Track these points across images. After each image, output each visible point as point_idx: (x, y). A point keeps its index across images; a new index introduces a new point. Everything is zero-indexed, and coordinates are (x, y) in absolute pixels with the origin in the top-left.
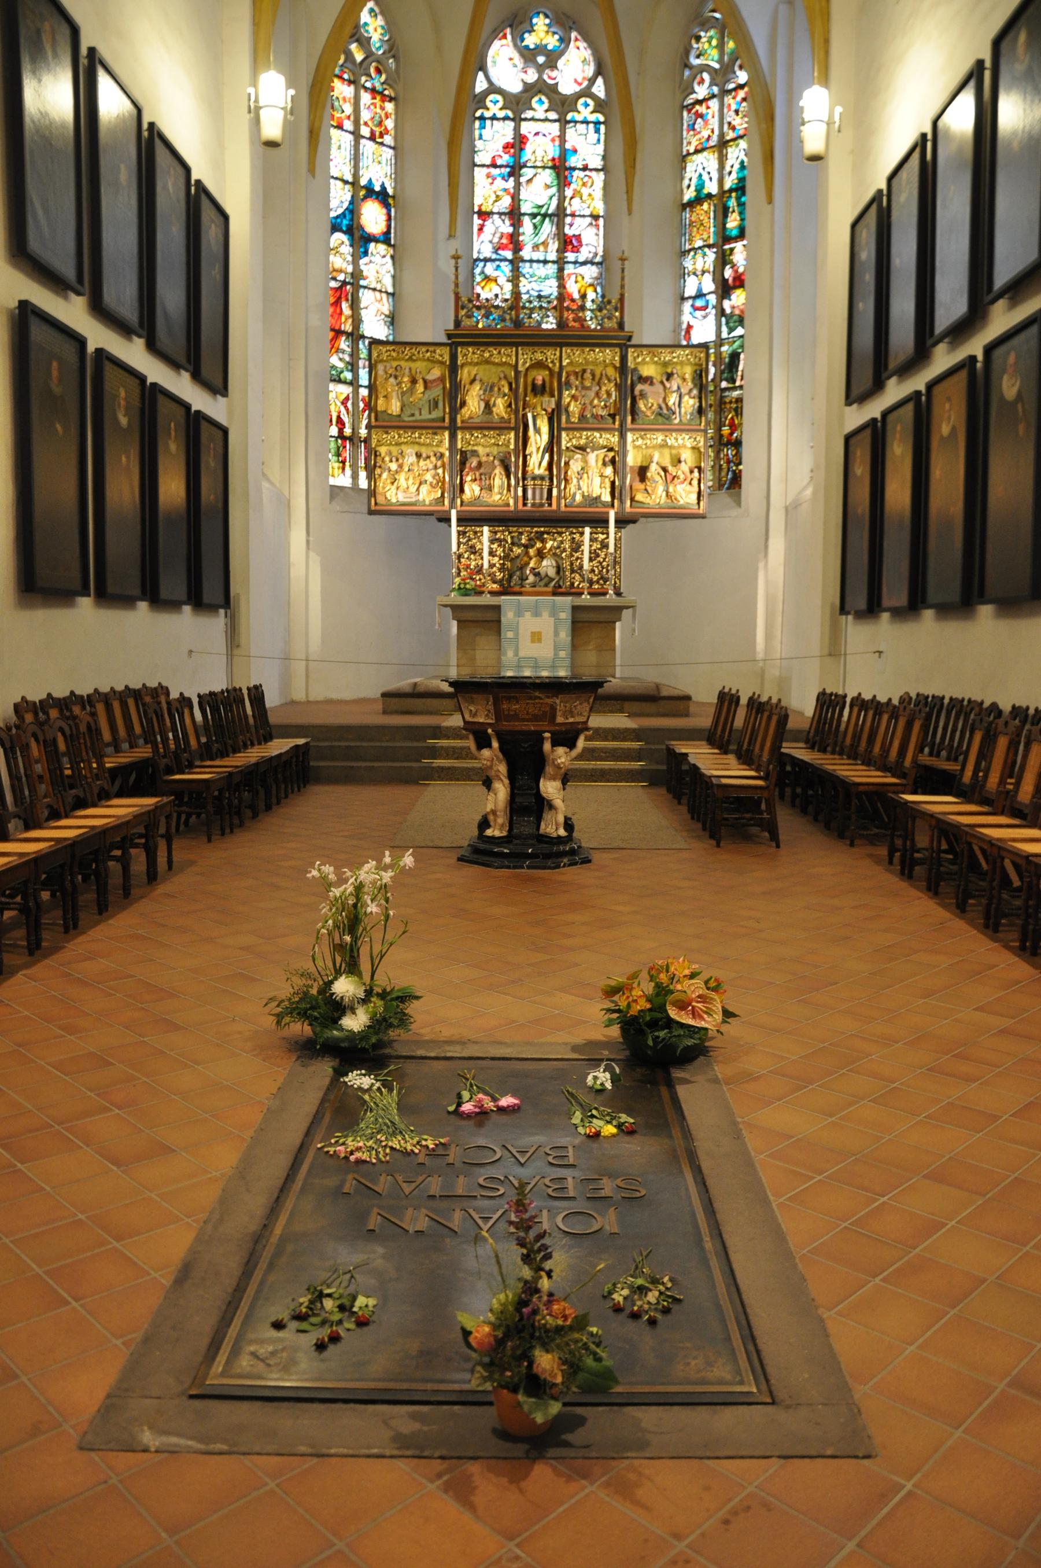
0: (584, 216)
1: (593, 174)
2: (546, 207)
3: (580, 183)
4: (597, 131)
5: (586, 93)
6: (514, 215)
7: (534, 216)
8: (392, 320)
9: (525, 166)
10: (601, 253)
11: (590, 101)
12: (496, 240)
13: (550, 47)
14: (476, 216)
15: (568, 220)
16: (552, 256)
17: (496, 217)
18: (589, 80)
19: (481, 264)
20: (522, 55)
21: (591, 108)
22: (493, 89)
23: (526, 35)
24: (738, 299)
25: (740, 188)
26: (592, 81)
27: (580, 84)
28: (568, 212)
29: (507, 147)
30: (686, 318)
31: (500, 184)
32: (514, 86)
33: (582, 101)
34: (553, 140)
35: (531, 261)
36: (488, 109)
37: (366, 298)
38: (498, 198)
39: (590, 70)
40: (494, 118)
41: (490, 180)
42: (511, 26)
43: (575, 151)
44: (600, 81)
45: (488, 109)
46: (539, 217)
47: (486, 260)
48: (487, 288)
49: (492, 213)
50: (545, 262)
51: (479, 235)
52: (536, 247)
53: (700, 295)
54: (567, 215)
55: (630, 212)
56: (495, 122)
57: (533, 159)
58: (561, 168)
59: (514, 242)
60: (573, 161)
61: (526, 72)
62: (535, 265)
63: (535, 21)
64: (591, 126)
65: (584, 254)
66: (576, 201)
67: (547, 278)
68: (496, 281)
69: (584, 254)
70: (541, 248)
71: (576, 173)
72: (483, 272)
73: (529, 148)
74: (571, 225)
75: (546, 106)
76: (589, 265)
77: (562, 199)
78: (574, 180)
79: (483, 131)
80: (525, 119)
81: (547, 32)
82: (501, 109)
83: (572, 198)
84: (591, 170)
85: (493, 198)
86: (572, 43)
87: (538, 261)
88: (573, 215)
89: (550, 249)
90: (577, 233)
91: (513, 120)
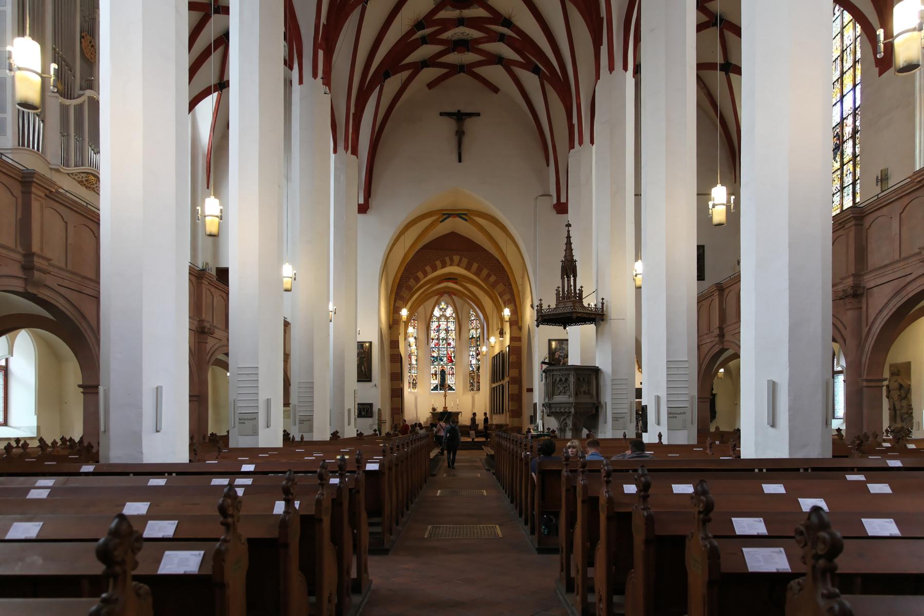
5: (452, 316)
6: (438, 339)
8: (416, 360)
16: (445, 347)
22: (434, 316)
24: (479, 357)
25: (479, 337)
26: (452, 314)
29: (437, 327)
30: (470, 359)
31: (436, 333)
32: (438, 316)
37: (413, 357)
39: (452, 312)
40: (434, 321)
52: (442, 345)
53: (473, 355)
55: (460, 339)
58: (447, 331)
59: (438, 344)
60: (449, 329)
65: (451, 346)
69: (451, 346)
77: (447, 335)
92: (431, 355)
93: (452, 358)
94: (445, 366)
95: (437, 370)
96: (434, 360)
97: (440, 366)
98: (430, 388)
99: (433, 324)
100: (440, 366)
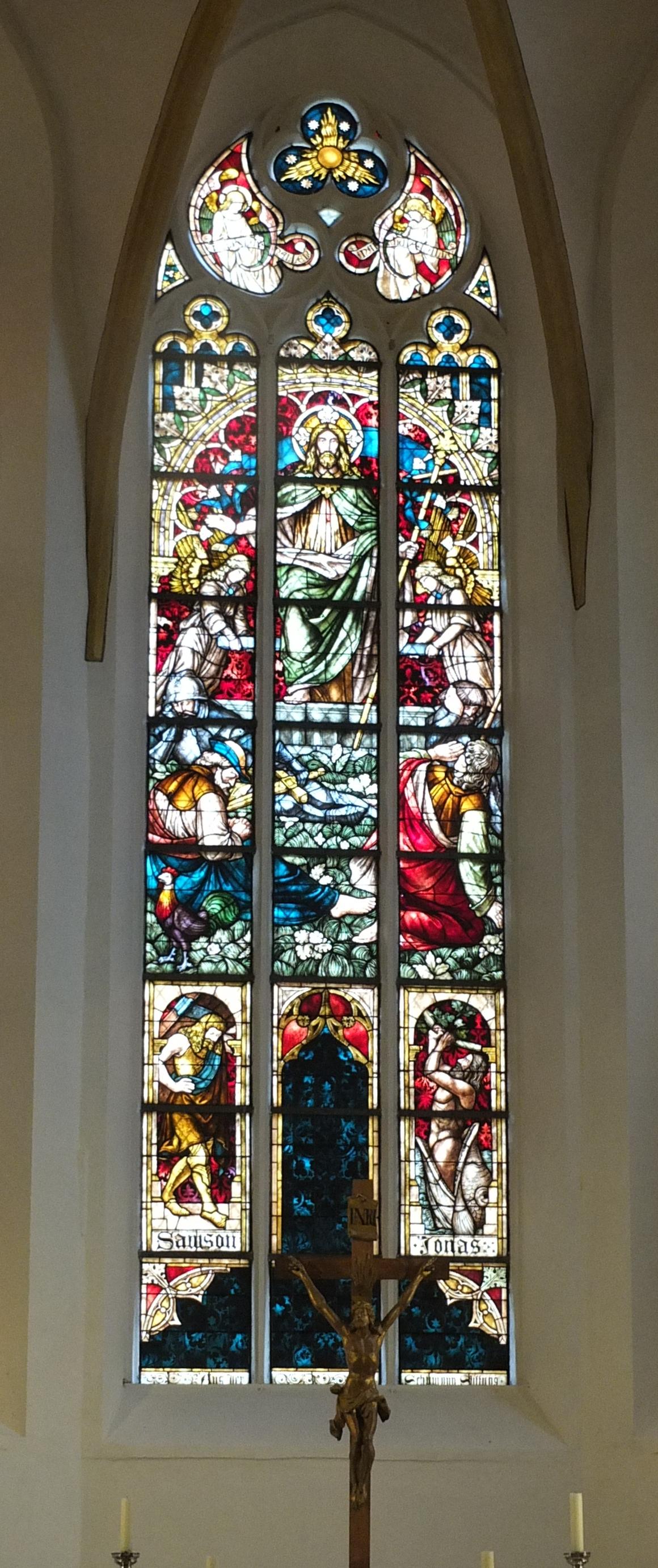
0: (450, 609)
1: (475, 502)
2: (345, 585)
3: (439, 524)
4: (480, 393)
7: (309, 608)
9: (288, 476)
10: (496, 706)
11: (459, 319)
12: (210, 669)
13: (353, 186)
14: (153, 606)
15: (408, 618)
17: (209, 608)
18: (455, 267)
19: (169, 734)
20: (277, 206)
21: (460, 338)
23: (291, 159)
26: (463, 269)
27: (431, 277)
28: (408, 597)
31: (221, 522)
33: (439, 317)
34: (362, 415)
35: (307, 726)
36: (190, 335)
38: (215, 560)
39: (459, 246)
40: (205, 356)
41: (194, 516)
42: (249, 136)
43: (424, 442)
44: (484, 272)
45: (190, 335)
46: (326, 612)
47: (183, 722)
48: (183, 801)
49: (204, 599)
50: (345, 729)
51: (161, 658)
52: (318, 691)
54: (402, 606)
55: (578, 600)
56: (208, 368)
57: (311, 461)
61: (290, 247)
62: (317, 738)
63: (313, 125)
64: (465, 379)
66: (426, 570)
67: (351, 771)
68: (210, 778)
70: (334, 694)
71: (425, 500)
72: (172, 754)
73: (300, 435)
74: (414, 633)
75: (340, 332)
76: (465, 739)
78: (421, 516)
79: (178, 391)
80: (291, 362)
81: (343, 151)
82: (222, 335)
83: (414, 563)
84: (467, 490)
85: (202, 553)
86: (411, 178)
87: (325, 727)
88: (420, 605)
89: (357, 697)
90: (432, 651)
91: (254, 362)
92: (152, 822)
93: (468, 871)
94: (365, 998)
95: (241, 1046)
96: (187, 903)
97: (287, 996)
98: (131, 1315)
99: (186, 393)
100: (287, 996)
